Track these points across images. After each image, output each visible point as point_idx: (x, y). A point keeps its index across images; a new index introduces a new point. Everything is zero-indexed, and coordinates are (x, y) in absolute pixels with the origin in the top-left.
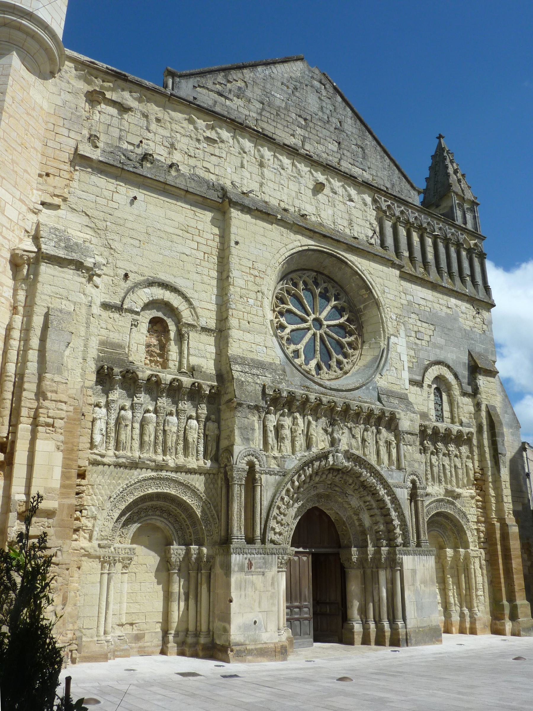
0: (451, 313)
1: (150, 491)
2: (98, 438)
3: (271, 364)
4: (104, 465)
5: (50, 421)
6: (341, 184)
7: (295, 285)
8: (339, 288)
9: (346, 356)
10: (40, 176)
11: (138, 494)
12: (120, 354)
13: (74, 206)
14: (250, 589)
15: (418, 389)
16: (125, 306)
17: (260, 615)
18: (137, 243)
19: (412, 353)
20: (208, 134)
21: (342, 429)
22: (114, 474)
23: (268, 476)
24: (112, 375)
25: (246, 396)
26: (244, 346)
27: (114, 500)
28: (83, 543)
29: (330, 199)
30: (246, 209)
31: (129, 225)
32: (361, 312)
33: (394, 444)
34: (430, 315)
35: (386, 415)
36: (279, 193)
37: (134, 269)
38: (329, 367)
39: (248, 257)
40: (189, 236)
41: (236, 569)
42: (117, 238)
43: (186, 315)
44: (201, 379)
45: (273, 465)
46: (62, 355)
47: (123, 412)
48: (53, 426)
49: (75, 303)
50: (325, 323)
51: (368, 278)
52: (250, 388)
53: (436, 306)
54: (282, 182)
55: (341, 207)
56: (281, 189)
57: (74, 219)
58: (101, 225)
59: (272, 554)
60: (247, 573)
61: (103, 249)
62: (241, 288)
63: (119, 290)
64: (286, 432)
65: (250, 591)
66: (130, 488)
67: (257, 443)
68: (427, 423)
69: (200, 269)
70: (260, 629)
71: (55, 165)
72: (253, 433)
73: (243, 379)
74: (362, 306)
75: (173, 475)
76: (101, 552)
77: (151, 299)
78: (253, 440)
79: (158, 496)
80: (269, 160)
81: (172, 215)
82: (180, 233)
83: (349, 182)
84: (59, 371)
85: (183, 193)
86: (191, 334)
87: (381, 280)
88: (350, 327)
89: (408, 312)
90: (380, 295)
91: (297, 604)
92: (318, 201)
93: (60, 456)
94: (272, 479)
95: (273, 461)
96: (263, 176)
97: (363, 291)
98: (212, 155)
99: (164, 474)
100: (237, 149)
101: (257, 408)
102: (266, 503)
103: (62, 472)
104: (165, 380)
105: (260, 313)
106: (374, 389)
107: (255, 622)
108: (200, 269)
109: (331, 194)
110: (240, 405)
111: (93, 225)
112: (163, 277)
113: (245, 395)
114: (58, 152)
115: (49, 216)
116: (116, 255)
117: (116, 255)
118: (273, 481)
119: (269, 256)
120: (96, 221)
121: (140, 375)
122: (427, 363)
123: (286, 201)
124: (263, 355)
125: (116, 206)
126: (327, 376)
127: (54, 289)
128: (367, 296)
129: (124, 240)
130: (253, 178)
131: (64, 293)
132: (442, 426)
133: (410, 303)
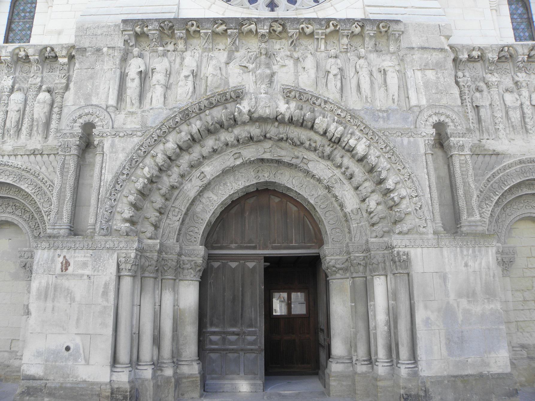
17: (78, 340)
41: (41, 271)
70: (76, 360)
107: (68, 349)
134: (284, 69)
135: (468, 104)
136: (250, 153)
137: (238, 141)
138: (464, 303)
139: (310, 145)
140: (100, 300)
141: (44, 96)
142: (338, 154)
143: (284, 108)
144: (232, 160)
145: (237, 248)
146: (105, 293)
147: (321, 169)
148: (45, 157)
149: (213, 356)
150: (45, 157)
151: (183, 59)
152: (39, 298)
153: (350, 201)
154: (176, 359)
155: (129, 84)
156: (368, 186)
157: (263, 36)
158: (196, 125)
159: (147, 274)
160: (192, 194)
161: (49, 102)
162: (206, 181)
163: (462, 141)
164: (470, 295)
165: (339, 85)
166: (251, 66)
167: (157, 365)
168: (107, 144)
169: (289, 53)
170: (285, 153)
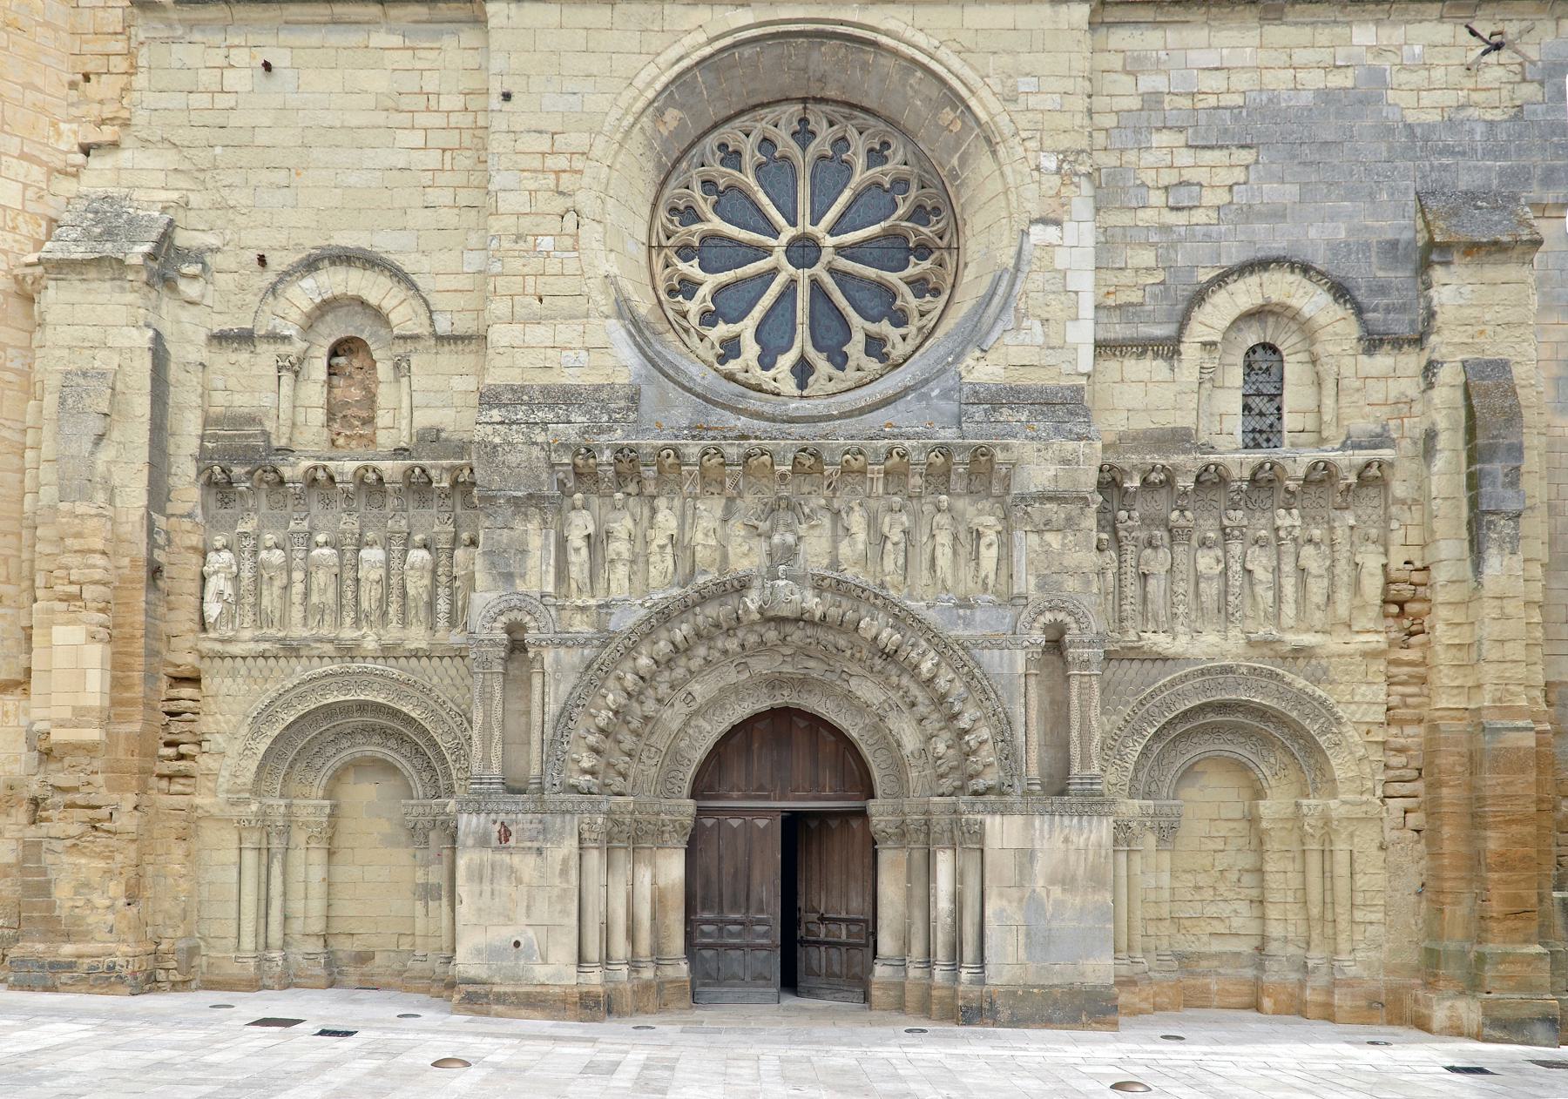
0: (1349, 83)
2: (213, 610)
3: (598, 388)
8: (882, 126)
13: (143, 135)
14: (504, 882)
15: (1160, 365)
17: (530, 932)
18: (280, 177)
19: (1147, 258)
22: (255, 673)
31: (262, 138)
32: (957, 177)
34: (1236, 119)
37: (281, 238)
41: (470, 842)
43: (403, 315)
44: (429, 457)
53: (1278, 80)
57: (149, 164)
58: (202, 158)
61: (213, 213)
63: (249, 298)
65: (504, 886)
68: (1178, 459)
69: (433, 196)
70: (529, 957)
72: (523, 562)
74: (955, 161)
75: (380, 666)
77: (318, 300)
78: (523, 576)
86: (414, 360)
89: (1137, 130)
102: (553, 708)
104: (342, 474)
107: (517, 944)
108: (433, 196)
111: (186, 166)
118: (576, 660)
120: (192, 151)
121: (287, 472)
122: (1204, 276)
128: (959, 124)
132: (1239, 461)
133: (1152, 100)
134: (817, 532)
135: (1129, 569)
136: (762, 666)
137: (743, 646)
138: (1057, 891)
139: (853, 655)
140: (557, 881)
141: (418, 556)
142: (892, 670)
143: (812, 603)
144: (734, 673)
145: (738, 799)
146: (564, 872)
147: (868, 691)
148: (436, 661)
149: (708, 953)
150: (436, 661)
151: (654, 511)
152: (470, 879)
153: (910, 740)
154: (658, 956)
155: (573, 558)
156: (933, 724)
157: (783, 476)
158: (682, 631)
159: (615, 844)
160: (675, 726)
161: (429, 566)
162: (695, 706)
163: (1086, 653)
164: (1066, 881)
165: (901, 561)
166: (764, 526)
167: (634, 964)
168: (549, 656)
169: (823, 502)
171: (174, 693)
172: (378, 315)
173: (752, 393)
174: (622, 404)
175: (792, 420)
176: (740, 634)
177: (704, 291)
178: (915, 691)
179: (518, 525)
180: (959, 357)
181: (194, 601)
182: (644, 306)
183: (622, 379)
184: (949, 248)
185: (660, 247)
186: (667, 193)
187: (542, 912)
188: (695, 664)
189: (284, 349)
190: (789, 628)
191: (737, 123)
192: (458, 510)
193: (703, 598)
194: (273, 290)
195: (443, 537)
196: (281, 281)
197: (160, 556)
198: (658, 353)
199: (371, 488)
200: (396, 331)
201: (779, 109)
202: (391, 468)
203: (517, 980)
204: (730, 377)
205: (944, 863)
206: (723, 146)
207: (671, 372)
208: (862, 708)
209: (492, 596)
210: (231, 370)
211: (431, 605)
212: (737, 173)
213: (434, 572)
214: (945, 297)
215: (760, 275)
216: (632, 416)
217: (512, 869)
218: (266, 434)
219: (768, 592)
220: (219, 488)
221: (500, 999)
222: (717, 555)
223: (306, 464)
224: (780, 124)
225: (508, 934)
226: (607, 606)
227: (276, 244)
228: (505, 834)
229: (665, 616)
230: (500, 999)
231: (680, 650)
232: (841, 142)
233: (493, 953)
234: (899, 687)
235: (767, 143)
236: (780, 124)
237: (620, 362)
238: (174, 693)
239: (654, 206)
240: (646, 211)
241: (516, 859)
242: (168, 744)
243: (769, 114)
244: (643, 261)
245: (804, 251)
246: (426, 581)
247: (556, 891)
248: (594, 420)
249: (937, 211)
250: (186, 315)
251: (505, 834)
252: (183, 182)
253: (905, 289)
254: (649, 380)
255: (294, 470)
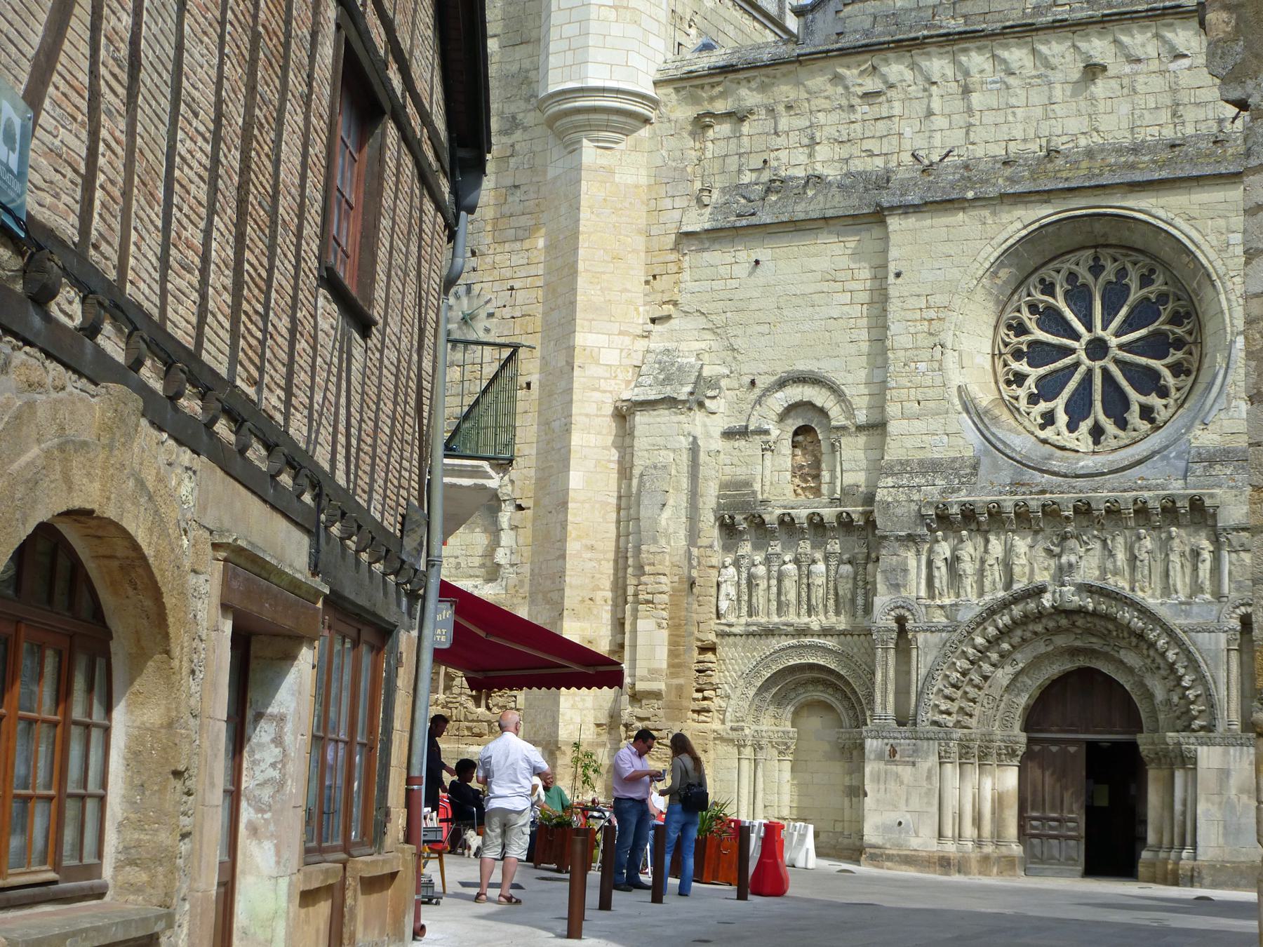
1: (792, 662)
3: (954, 460)
4: (735, 635)
5: (649, 597)
6: (1149, 35)
7: (1049, 289)
8: (1148, 260)
9: (1163, 393)
10: (647, 282)
11: (775, 668)
12: (744, 495)
13: (686, 309)
16: (751, 428)
17: (908, 816)
18: (765, 329)
20: (871, 84)
21: (1086, 543)
23: (928, 634)
24: (742, 521)
25: (894, 524)
26: (910, 443)
27: (748, 677)
28: (716, 725)
29: (1126, 81)
30: (907, 209)
33: (1206, 555)
35: (1179, 504)
36: (1005, 128)
37: (763, 368)
38: (1122, 424)
39: (918, 291)
40: (839, 286)
41: (872, 757)
42: (740, 332)
43: (837, 415)
45: (940, 619)
46: (655, 521)
47: (753, 570)
48: (652, 602)
49: (674, 451)
50: (1113, 342)
51: (1184, 230)
52: (899, 511)
54: (1013, 101)
55: (1158, 83)
56: (1011, 118)
57: (690, 326)
58: (719, 320)
59: (928, 739)
60: (887, 763)
62: (906, 350)
64: (968, 567)
65: (892, 785)
66: (764, 662)
67: (916, 586)
70: (907, 832)
71: (661, 260)
73: (890, 499)
74: (1195, 285)
76: (734, 735)
78: (905, 586)
79: (812, 667)
80: (982, 71)
81: (814, 263)
82: (825, 286)
83: (1168, 20)
84: (655, 541)
85: (822, 222)
87: (1222, 222)
88: (1174, 333)
90: (1212, 255)
91: (1035, 814)
92: (1093, 100)
93: (664, 634)
94: (935, 638)
95: (939, 612)
96: (969, 111)
97: (1185, 259)
98: (876, 120)
99: (807, 640)
100: (921, 82)
101: (911, 538)
102: (923, 672)
103: (670, 651)
105: (938, 381)
106: (1178, 457)
107: (900, 823)
109: (1127, 69)
110: (885, 538)
111: (710, 325)
112: (802, 366)
113: (892, 521)
114: (662, 238)
115: (662, 334)
116: (739, 357)
117: (739, 357)
118: (937, 640)
119: (955, 273)
120: (713, 317)
121: (767, 518)
123: (1019, 134)
124: (941, 449)
125: (734, 283)
126: (1114, 443)
127: (650, 440)
129: (749, 331)
130: (954, 123)
131: (661, 441)
134: (1091, 553)
140: (925, 783)
146: (929, 778)
151: (987, 541)
152: (872, 781)
153: (1160, 694)
155: (936, 573)
158: (1003, 620)
168: (921, 637)
170: (1096, 643)
171: (701, 657)
172: (822, 412)
173: (1059, 453)
174: (968, 471)
175: (1077, 476)
176: (1044, 621)
177: (1030, 382)
178: (1159, 660)
179: (902, 552)
180: (1189, 428)
181: (714, 600)
182: (985, 396)
183: (969, 453)
184: (1195, 343)
185: (1001, 354)
186: (1005, 317)
187: (915, 803)
188: (1016, 640)
189: (765, 438)
190: (1075, 617)
191: (1051, 266)
192: (870, 536)
193: (1016, 599)
194: (759, 401)
195: (860, 556)
196: (764, 395)
197: (695, 573)
198: (993, 434)
199: (818, 526)
200: (834, 423)
201: (1078, 254)
202: (829, 513)
203: (900, 846)
204: (1045, 442)
205: (1179, 776)
206: (1042, 281)
207: (1001, 446)
208: (1130, 670)
209: (886, 599)
210: (736, 453)
211: (853, 601)
212: (1051, 300)
213: (855, 578)
214: (1193, 377)
215: (1067, 367)
216: (973, 480)
217: (897, 776)
218: (754, 493)
219: (1057, 595)
220: (729, 529)
221: (890, 858)
222: (1027, 570)
223: (779, 512)
224: (1080, 265)
225: (891, 817)
226: (956, 605)
227: (760, 371)
228: (893, 752)
229: (992, 612)
230: (890, 858)
231: (1003, 633)
232: (1122, 273)
233: (886, 829)
234: (1149, 656)
235: (1072, 277)
236: (1080, 265)
237: (968, 441)
238: (701, 657)
239: (996, 327)
240: (990, 333)
241: (900, 768)
242: (698, 691)
243: (1073, 258)
244: (988, 366)
245: (1098, 348)
246: (850, 585)
247: (924, 790)
248: (950, 482)
249: (1188, 315)
250: (710, 420)
251: (893, 752)
252: (709, 335)
253: (1166, 373)
254: (986, 452)
255: (772, 516)
